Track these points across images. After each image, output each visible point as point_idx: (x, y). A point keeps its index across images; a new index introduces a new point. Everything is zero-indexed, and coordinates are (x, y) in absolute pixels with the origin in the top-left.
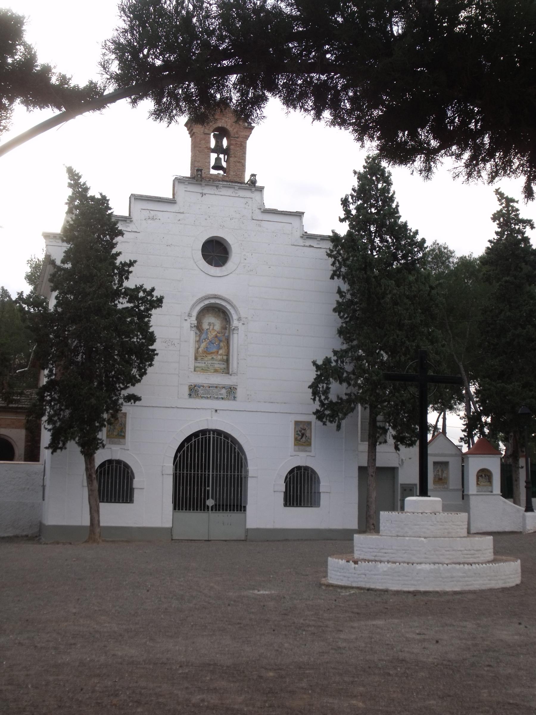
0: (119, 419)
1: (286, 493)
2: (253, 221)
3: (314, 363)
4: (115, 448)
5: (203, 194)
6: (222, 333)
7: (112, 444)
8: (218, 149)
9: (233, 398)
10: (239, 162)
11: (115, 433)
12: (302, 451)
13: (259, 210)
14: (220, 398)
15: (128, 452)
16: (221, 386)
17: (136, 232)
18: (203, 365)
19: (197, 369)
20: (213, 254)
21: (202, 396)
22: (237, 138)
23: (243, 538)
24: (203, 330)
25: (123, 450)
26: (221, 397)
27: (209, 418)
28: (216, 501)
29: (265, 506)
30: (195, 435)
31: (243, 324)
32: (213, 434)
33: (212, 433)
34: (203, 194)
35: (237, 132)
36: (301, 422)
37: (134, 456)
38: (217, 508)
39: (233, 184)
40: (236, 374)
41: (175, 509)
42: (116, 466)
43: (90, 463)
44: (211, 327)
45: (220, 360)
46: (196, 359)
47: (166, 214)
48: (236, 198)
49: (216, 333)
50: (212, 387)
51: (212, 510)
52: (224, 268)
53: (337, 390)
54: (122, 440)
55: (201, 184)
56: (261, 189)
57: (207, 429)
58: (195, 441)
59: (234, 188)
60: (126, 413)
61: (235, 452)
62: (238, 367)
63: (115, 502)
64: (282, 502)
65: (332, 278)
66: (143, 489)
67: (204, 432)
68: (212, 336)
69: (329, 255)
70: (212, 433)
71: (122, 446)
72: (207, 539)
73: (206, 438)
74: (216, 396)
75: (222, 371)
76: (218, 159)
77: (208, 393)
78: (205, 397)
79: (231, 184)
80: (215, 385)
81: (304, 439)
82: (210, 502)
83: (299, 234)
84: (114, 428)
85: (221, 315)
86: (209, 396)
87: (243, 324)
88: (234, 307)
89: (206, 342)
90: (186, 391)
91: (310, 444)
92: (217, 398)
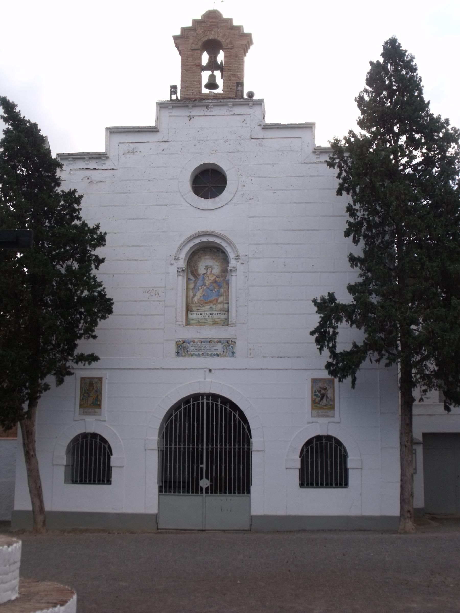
0: (94, 385)
1: (301, 471)
2: (253, 140)
3: (314, 301)
4: (90, 419)
5: (190, 118)
6: (222, 277)
7: (87, 414)
8: (213, 65)
9: (231, 354)
10: (235, 76)
11: (90, 402)
12: (322, 416)
13: (259, 127)
14: (215, 355)
15: (105, 424)
16: (216, 340)
17: (113, 169)
18: (200, 316)
19: (192, 322)
20: (208, 185)
21: (192, 353)
22: (231, 48)
23: (247, 528)
24: (199, 275)
25: (99, 422)
26: (216, 353)
27: (203, 380)
28: (211, 481)
29: (275, 487)
30: (186, 400)
31: (242, 263)
32: (208, 399)
33: (205, 397)
34: (190, 118)
35: (231, 43)
36: (320, 380)
37: (112, 428)
38: (211, 490)
39: (225, 101)
40: (234, 324)
41: (160, 491)
42: (91, 441)
43: (28, 438)
44: (209, 271)
45: (221, 310)
46: (188, 309)
47: (147, 145)
48: (231, 117)
49: (215, 277)
50: (204, 342)
51: (207, 493)
52: (217, 199)
53: (348, 336)
54: (97, 410)
55: (187, 106)
56: (260, 103)
57: (200, 393)
58: (185, 409)
59: (228, 105)
60: (102, 378)
61: (235, 421)
62: (237, 316)
63: (90, 482)
64: (297, 481)
65: (339, 193)
66: (123, 467)
67: (196, 397)
68: (210, 281)
69: (331, 165)
70: (205, 397)
71: (97, 417)
72: (200, 528)
73: (198, 404)
74: (210, 353)
75: (222, 322)
76: (212, 77)
77: (198, 350)
78: (196, 355)
79: (222, 101)
80: (209, 340)
81: (324, 401)
82: (204, 483)
83: (311, 149)
84: (89, 396)
85: (221, 255)
86: (201, 353)
87: (242, 263)
88: (230, 243)
89: (202, 289)
90: (173, 348)
91: (332, 408)
92: (211, 355)
